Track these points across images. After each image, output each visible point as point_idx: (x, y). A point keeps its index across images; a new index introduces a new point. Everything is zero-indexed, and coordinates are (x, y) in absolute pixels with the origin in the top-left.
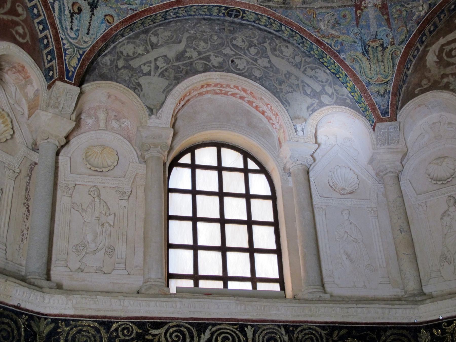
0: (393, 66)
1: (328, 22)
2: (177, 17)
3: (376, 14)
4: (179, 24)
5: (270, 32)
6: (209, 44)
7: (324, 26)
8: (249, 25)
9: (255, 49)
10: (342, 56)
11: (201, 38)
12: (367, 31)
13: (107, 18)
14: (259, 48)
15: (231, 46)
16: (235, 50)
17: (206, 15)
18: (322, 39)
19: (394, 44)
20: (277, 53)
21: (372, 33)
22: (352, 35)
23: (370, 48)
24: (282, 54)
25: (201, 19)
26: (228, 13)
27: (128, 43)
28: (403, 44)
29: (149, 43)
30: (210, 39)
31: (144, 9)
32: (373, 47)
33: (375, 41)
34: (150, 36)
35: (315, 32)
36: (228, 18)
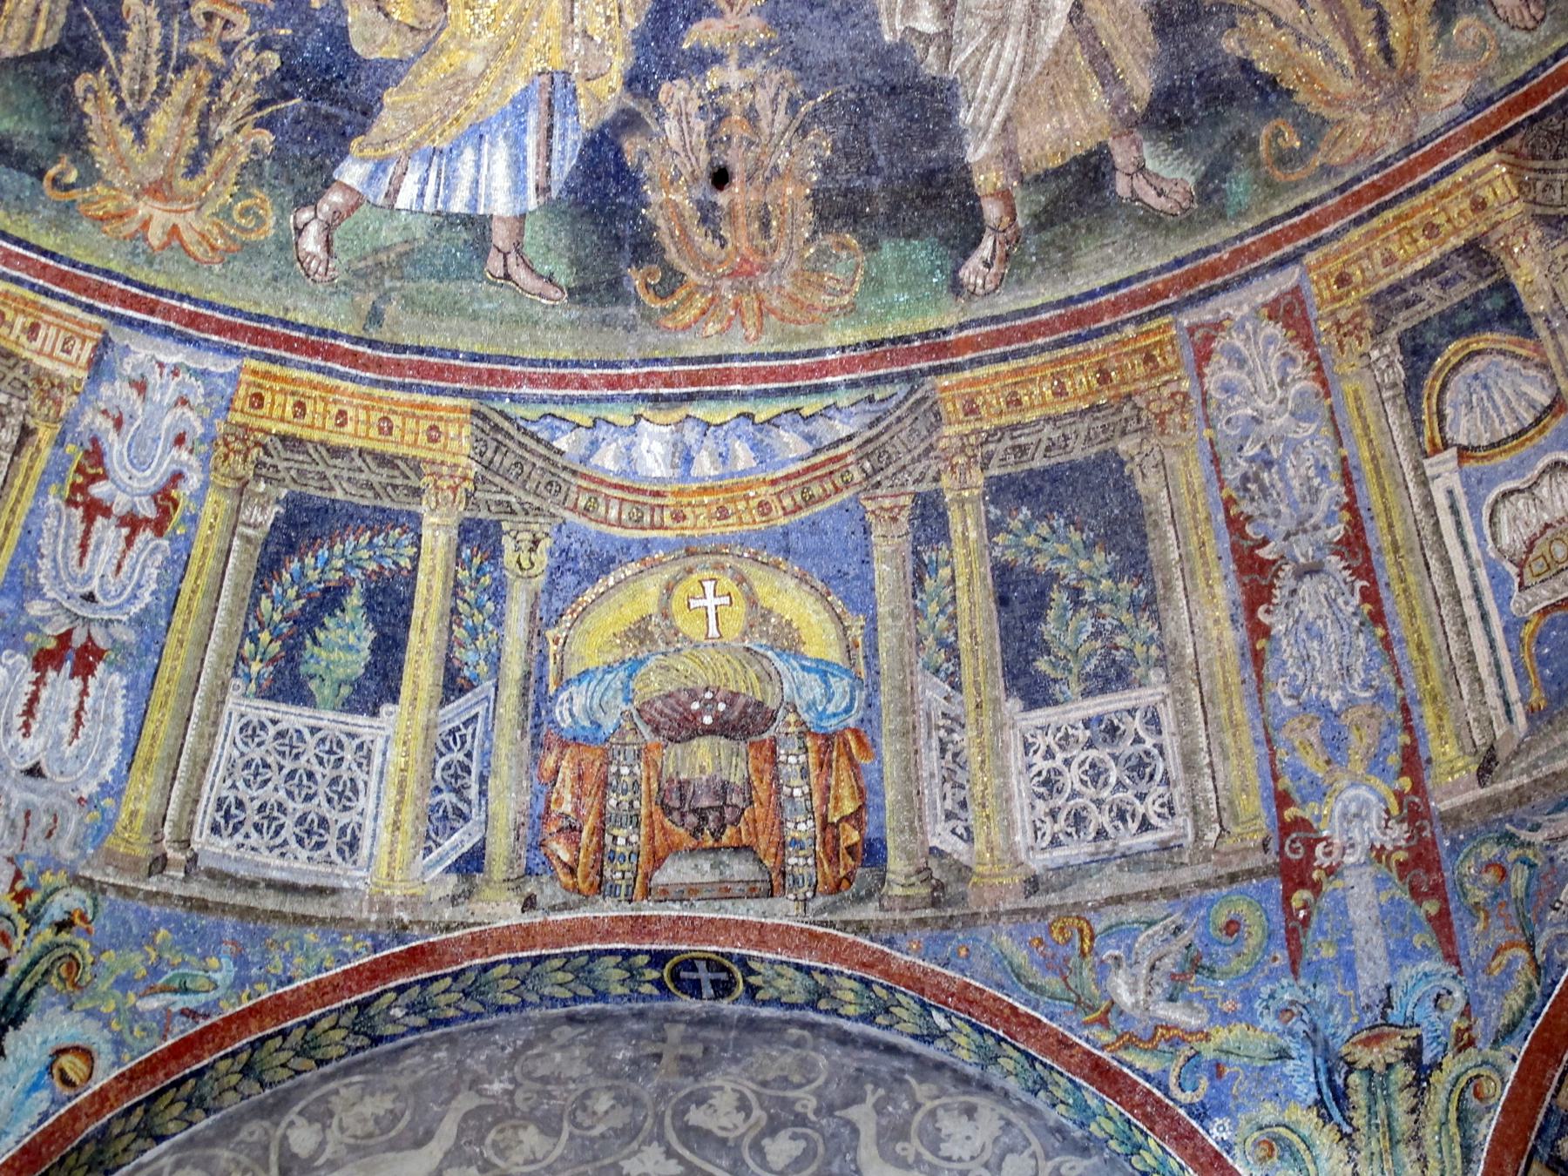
0: (1467, 1160)
1: (1153, 968)
2: (433, 1023)
3: (1384, 898)
4: (442, 1054)
5: (892, 1049)
6: (565, 1136)
7: (1133, 991)
8: (789, 1022)
9: (794, 1137)
10: (1216, 1133)
11: (532, 1109)
12: (1339, 989)
13: (66, 1061)
14: (821, 1131)
15: (672, 1137)
16: (687, 1154)
17: (577, 999)
18: (1122, 1054)
19: (1471, 1043)
20: (912, 1147)
21: (1364, 1000)
22: (1269, 1021)
23: (1355, 1079)
24: (935, 1151)
25: (555, 1022)
26: (675, 977)
27: (178, 1165)
28: (1518, 1036)
29: (273, 1157)
30: (573, 1112)
31: (247, 1004)
32: (1369, 1071)
33: (1378, 1039)
34: (291, 1124)
35: (1087, 1025)
36: (685, 1003)
